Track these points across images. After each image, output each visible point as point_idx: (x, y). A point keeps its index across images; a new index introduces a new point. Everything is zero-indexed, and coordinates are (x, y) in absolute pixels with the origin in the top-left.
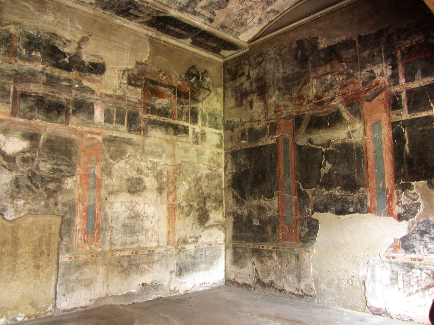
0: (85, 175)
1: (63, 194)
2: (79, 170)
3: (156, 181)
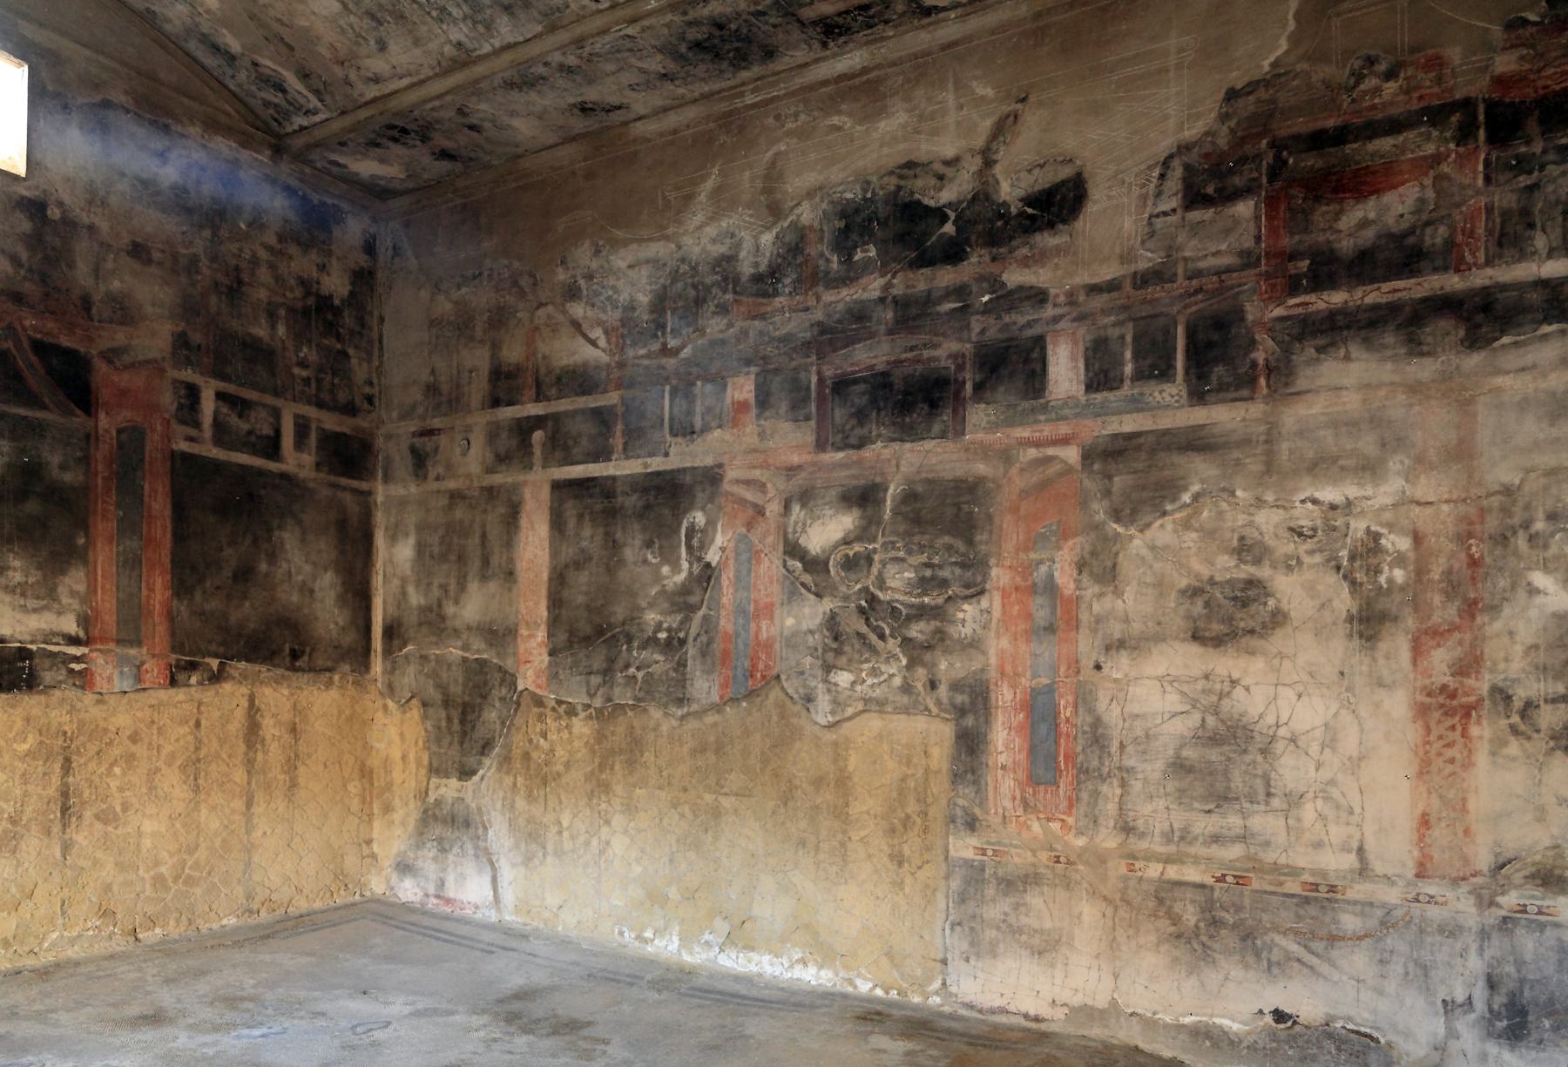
0: (1017, 589)
1: (951, 654)
2: (999, 575)
3: (1345, 585)
